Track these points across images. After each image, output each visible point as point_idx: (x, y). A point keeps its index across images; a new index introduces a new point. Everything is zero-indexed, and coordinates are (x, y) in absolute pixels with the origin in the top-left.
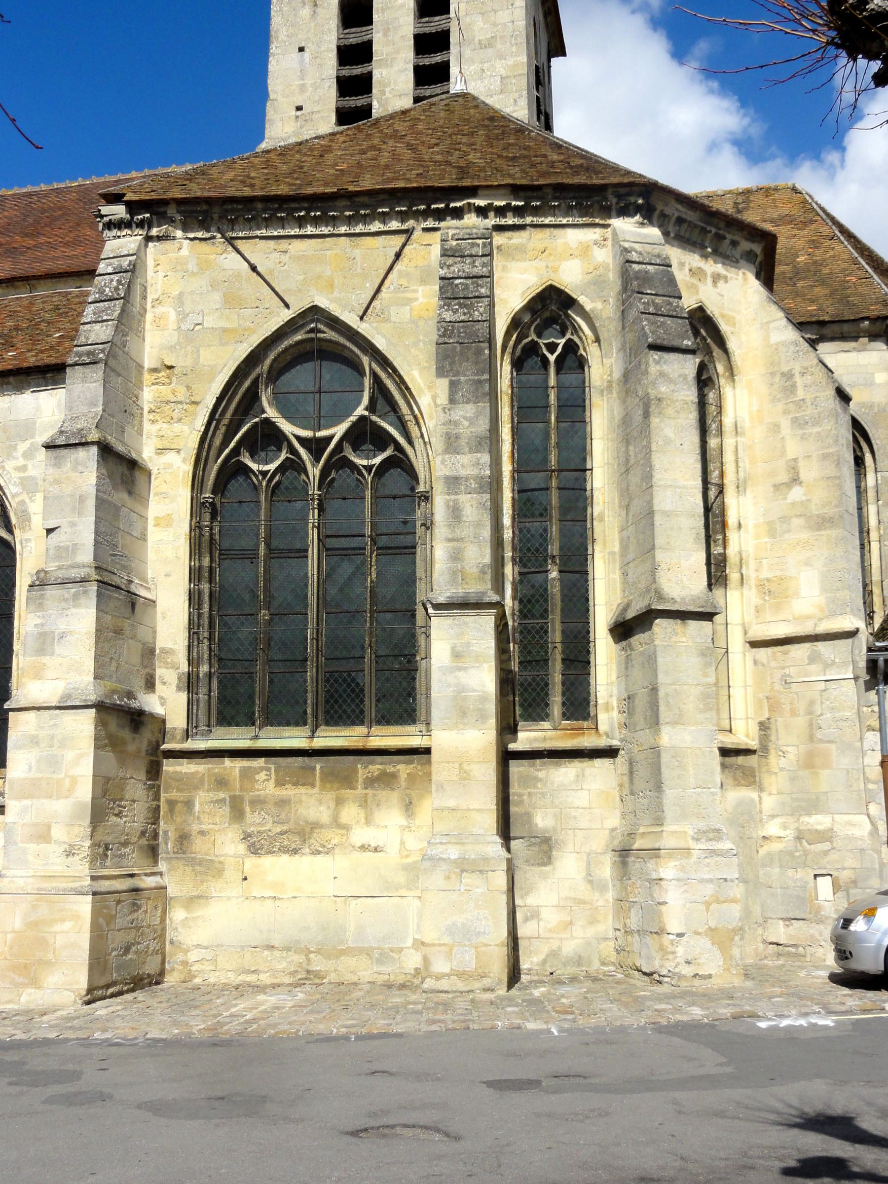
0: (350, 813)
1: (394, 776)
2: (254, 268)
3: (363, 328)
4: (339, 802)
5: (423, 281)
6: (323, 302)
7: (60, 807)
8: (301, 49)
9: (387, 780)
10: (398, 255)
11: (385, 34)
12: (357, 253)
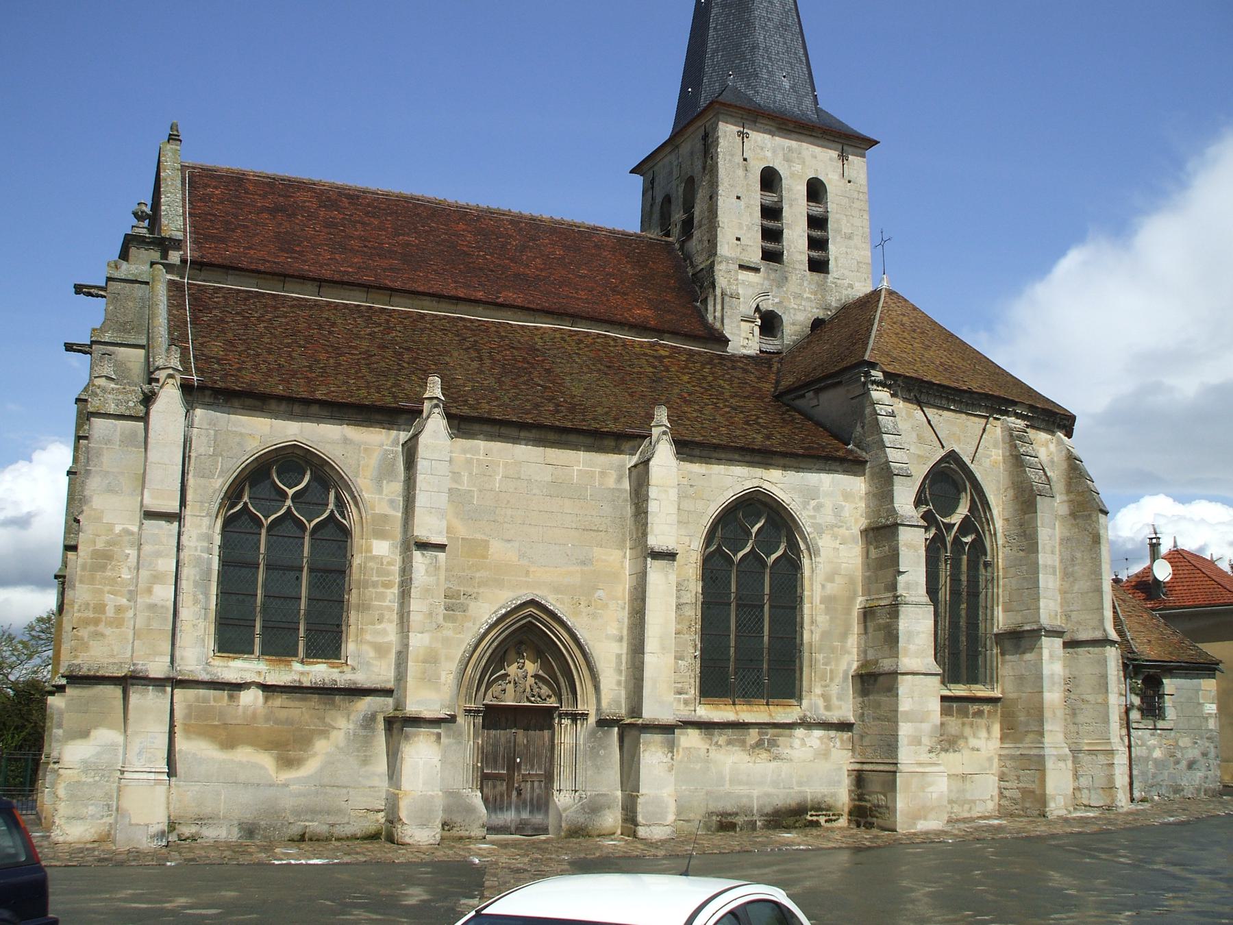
0: (967, 731)
1: (982, 712)
2: (929, 422)
3: (972, 467)
4: (963, 724)
5: (995, 446)
6: (957, 450)
7: (926, 727)
8: (738, 198)
9: (979, 714)
10: (984, 430)
11: (791, 206)
12: (969, 423)
